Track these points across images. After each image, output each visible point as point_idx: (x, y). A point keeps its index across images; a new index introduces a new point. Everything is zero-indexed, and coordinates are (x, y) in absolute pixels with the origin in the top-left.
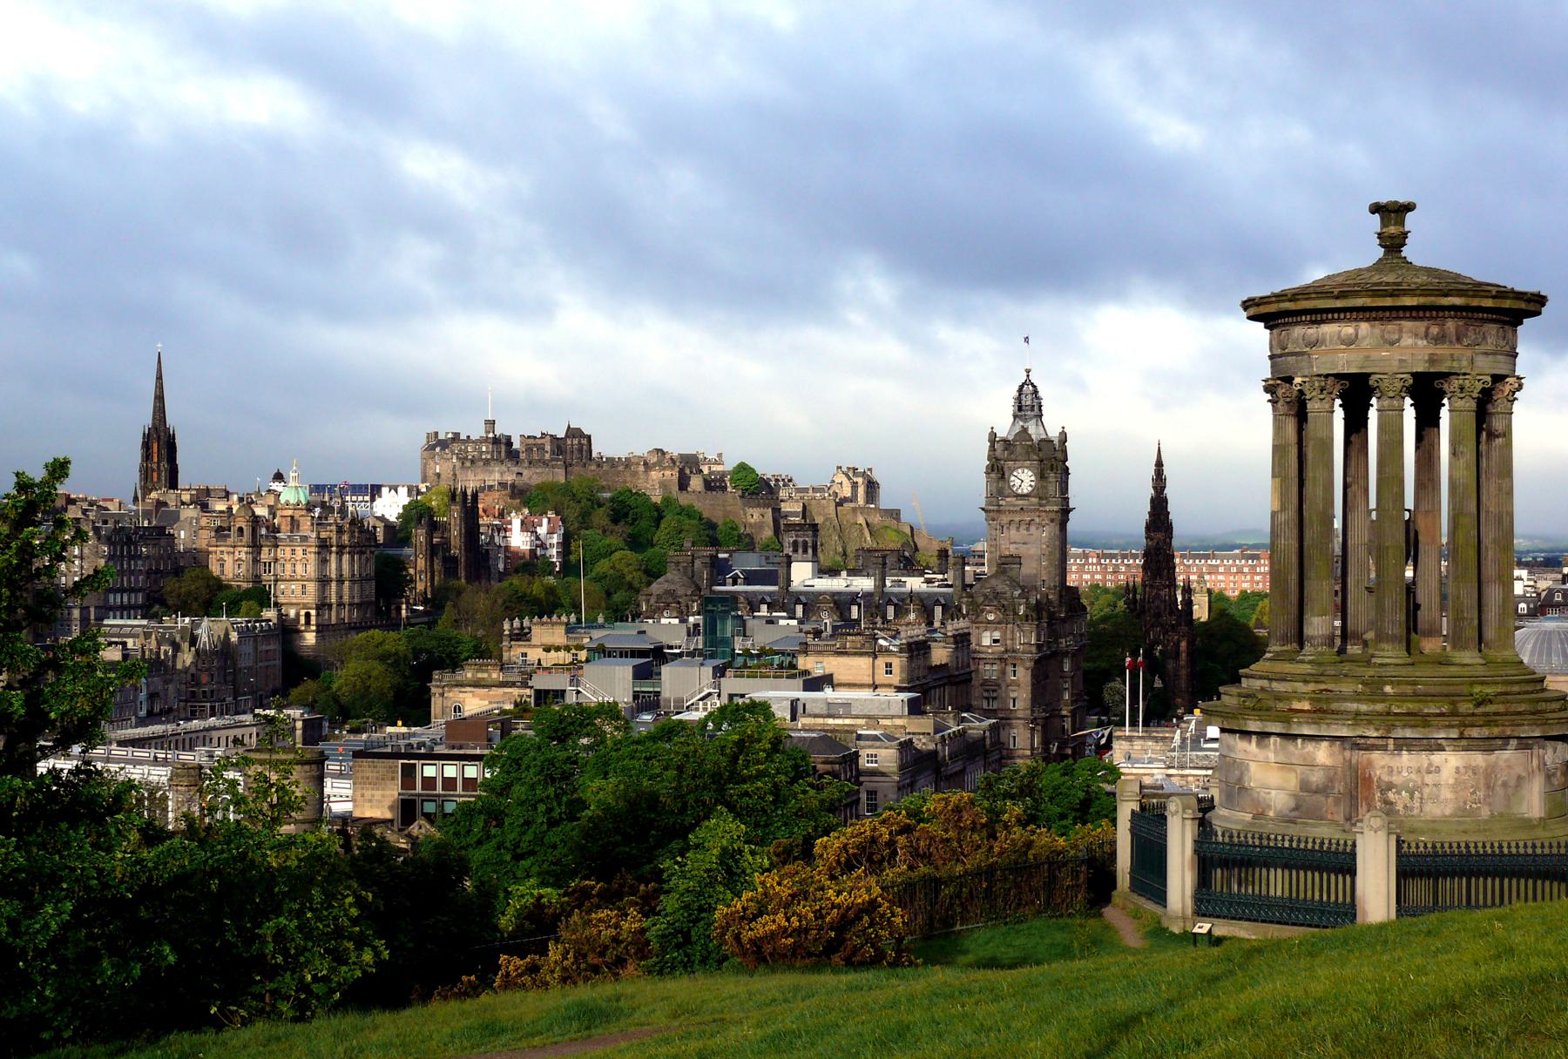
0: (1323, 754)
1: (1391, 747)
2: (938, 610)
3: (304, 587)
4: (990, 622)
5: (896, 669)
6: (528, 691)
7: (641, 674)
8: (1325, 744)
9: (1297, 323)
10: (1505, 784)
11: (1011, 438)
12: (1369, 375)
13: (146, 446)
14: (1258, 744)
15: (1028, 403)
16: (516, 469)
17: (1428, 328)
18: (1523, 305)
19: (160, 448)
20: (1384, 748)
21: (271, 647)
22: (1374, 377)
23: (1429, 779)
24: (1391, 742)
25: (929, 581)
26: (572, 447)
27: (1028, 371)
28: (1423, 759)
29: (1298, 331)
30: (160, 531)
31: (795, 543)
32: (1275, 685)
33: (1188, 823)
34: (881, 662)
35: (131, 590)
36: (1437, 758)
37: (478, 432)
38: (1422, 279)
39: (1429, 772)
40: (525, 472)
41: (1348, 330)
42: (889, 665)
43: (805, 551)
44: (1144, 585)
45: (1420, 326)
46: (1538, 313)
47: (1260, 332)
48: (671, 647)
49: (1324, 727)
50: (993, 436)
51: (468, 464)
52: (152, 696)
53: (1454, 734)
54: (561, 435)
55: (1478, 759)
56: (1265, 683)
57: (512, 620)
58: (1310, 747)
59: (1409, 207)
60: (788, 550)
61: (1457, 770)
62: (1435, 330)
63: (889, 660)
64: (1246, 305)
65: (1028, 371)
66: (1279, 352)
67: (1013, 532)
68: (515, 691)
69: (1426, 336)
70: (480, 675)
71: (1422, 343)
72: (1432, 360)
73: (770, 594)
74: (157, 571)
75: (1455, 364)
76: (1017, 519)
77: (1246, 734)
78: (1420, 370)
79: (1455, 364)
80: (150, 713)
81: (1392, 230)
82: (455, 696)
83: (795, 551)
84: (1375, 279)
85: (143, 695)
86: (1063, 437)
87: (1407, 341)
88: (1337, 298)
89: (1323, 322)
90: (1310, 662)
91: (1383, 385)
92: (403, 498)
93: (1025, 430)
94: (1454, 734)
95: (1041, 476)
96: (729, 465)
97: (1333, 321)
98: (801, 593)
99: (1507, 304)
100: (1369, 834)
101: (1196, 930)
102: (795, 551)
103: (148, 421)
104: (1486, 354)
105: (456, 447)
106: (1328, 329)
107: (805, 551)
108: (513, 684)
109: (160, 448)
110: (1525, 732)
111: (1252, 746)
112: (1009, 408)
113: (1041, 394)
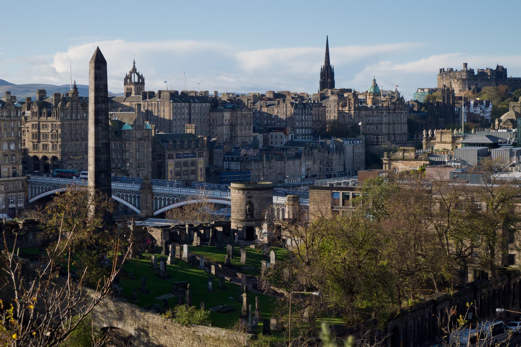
3: (377, 127)
6: (428, 162)
7: (481, 154)
13: (323, 75)
19: (327, 75)
21: (361, 151)
26: (500, 73)
30: (320, 105)
35: (306, 128)
40: (479, 84)
52: (307, 170)
54: (494, 68)
57: (427, 131)
74: (319, 121)
80: (307, 177)
82: (395, 164)
85: (303, 170)
103: (323, 63)
105: (452, 74)
109: (327, 75)
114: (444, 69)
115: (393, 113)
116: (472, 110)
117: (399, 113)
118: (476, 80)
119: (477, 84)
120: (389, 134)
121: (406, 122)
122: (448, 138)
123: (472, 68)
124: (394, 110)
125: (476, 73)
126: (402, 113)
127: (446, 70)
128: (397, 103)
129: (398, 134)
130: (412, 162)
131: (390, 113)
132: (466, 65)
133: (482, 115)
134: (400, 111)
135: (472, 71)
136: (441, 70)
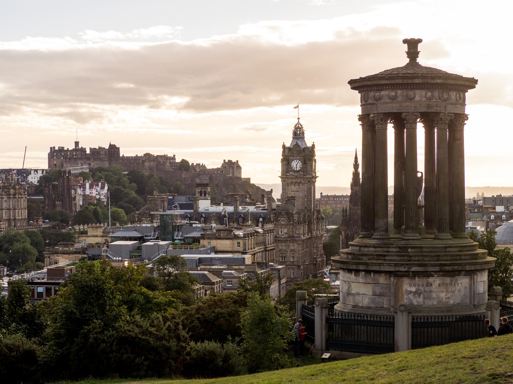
0: (382, 279)
1: (411, 275)
2: (261, 219)
4: (283, 225)
5: (242, 245)
6: (86, 256)
8: (383, 274)
9: (371, 91)
10: (459, 290)
11: (291, 147)
12: (401, 113)
14: (355, 275)
15: (298, 133)
16: (88, 162)
17: (426, 93)
18: (467, 83)
20: (408, 276)
22: (403, 114)
23: (427, 289)
24: (411, 273)
25: (257, 208)
27: (299, 119)
28: (424, 281)
29: (372, 94)
31: (201, 191)
32: (362, 249)
33: (324, 309)
34: (235, 242)
36: (431, 280)
37: (72, 147)
38: (425, 71)
39: (427, 286)
40: (92, 163)
41: (393, 94)
42: (239, 243)
43: (205, 195)
44: (350, 209)
45: (423, 92)
46: (475, 87)
47: (357, 95)
48: (146, 236)
49: (382, 267)
50: (284, 147)
51: (68, 160)
53: (437, 269)
54: (107, 147)
55: (448, 280)
56: (357, 248)
58: (377, 276)
59: (420, 41)
60: (198, 195)
61: (439, 285)
62: (429, 94)
63: (239, 241)
64: (351, 82)
65: (299, 119)
66: (364, 103)
67: (293, 187)
68: (80, 256)
69: (426, 97)
70: (65, 249)
71: (424, 99)
72: (428, 106)
73: (190, 213)
75: (438, 109)
76: (294, 181)
77: (350, 271)
78: (423, 111)
79: (438, 109)
81: (412, 51)
83: (201, 195)
84: (404, 72)
86: (313, 146)
87: (417, 98)
88: (387, 79)
89: (382, 90)
90: (377, 239)
91: (407, 118)
92: (40, 174)
93: (297, 144)
94: (437, 269)
95: (304, 163)
96: (178, 160)
97: (386, 89)
98: (203, 213)
99: (460, 82)
100: (400, 314)
101: (324, 356)
102: (201, 195)
104: (452, 104)
106: (383, 93)
107: (205, 195)
108: (79, 253)
110: (468, 268)
111: (352, 276)
112: (291, 135)
113: (304, 129)
114: (54, 147)
115: (14, 198)
116: (88, 192)
117: (19, 198)
118: (88, 159)
119: (90, 164)
120: (9, 220)
121: (26, 207)
122: (99, 232)
123: (84, 147)
124: (15, 195)
125: (88, 152)
126: (22, 198)
127: (57, 148)
128: (17, 187)
129: (19, 220)
130: (71, 256)
131: (10, 198)
132: (77, 143)
133: (98, 197)
134: (20, 196)
135: (83, 150)
136: (51, 148)
